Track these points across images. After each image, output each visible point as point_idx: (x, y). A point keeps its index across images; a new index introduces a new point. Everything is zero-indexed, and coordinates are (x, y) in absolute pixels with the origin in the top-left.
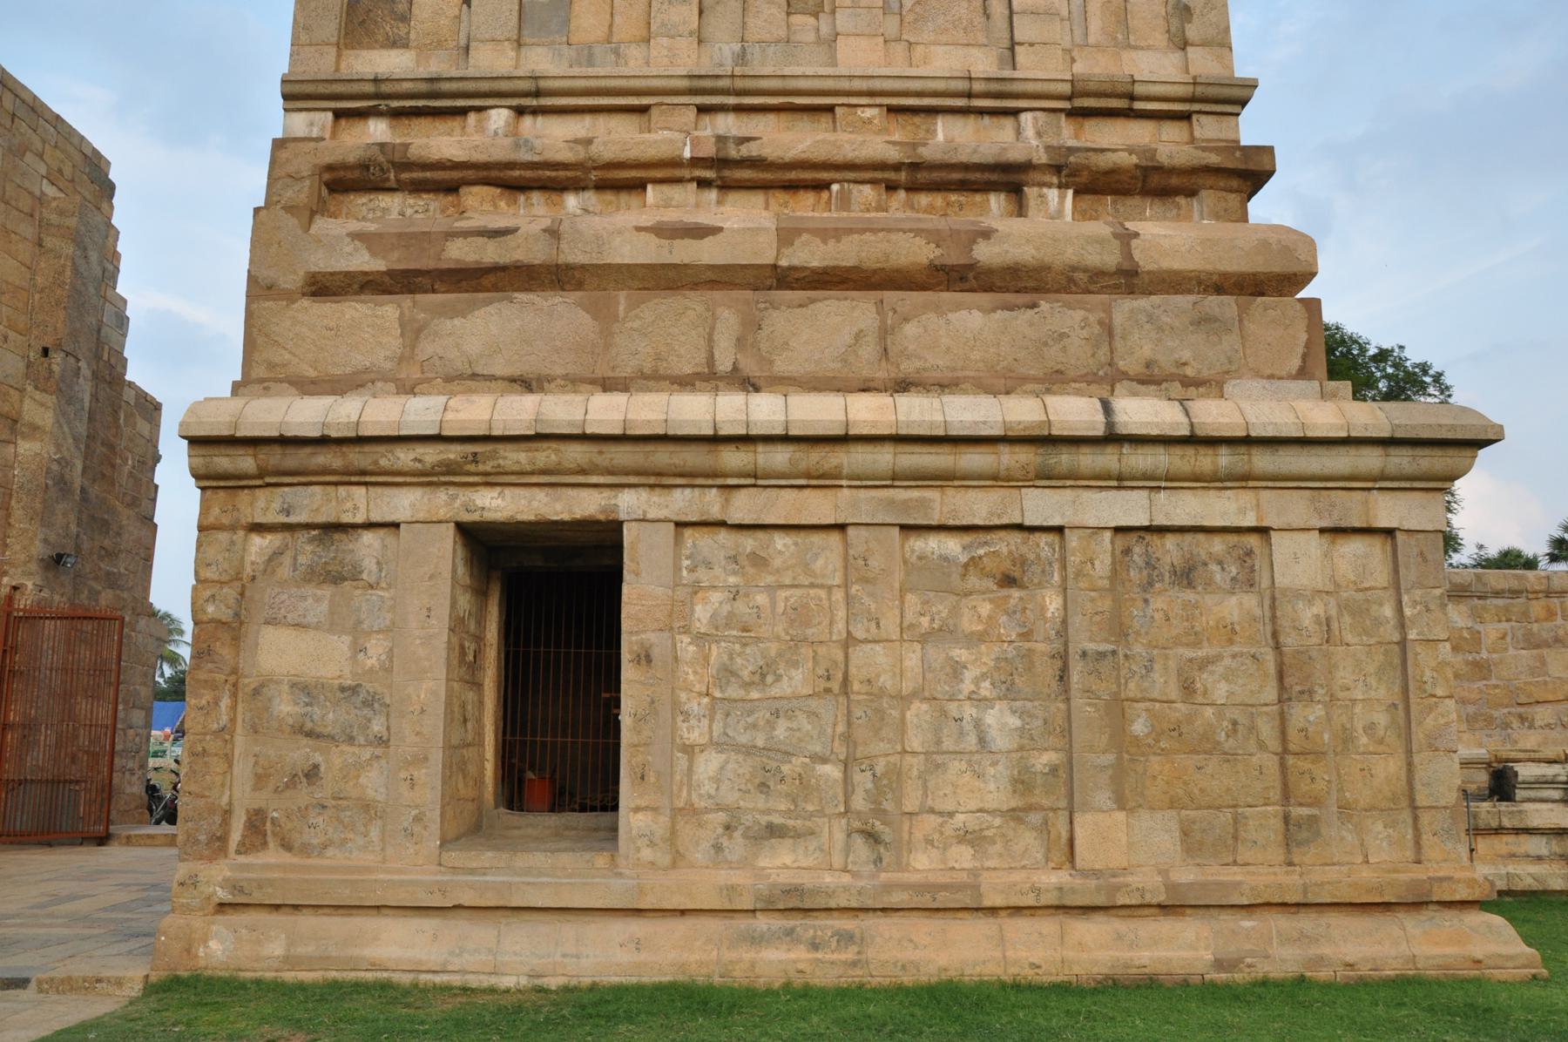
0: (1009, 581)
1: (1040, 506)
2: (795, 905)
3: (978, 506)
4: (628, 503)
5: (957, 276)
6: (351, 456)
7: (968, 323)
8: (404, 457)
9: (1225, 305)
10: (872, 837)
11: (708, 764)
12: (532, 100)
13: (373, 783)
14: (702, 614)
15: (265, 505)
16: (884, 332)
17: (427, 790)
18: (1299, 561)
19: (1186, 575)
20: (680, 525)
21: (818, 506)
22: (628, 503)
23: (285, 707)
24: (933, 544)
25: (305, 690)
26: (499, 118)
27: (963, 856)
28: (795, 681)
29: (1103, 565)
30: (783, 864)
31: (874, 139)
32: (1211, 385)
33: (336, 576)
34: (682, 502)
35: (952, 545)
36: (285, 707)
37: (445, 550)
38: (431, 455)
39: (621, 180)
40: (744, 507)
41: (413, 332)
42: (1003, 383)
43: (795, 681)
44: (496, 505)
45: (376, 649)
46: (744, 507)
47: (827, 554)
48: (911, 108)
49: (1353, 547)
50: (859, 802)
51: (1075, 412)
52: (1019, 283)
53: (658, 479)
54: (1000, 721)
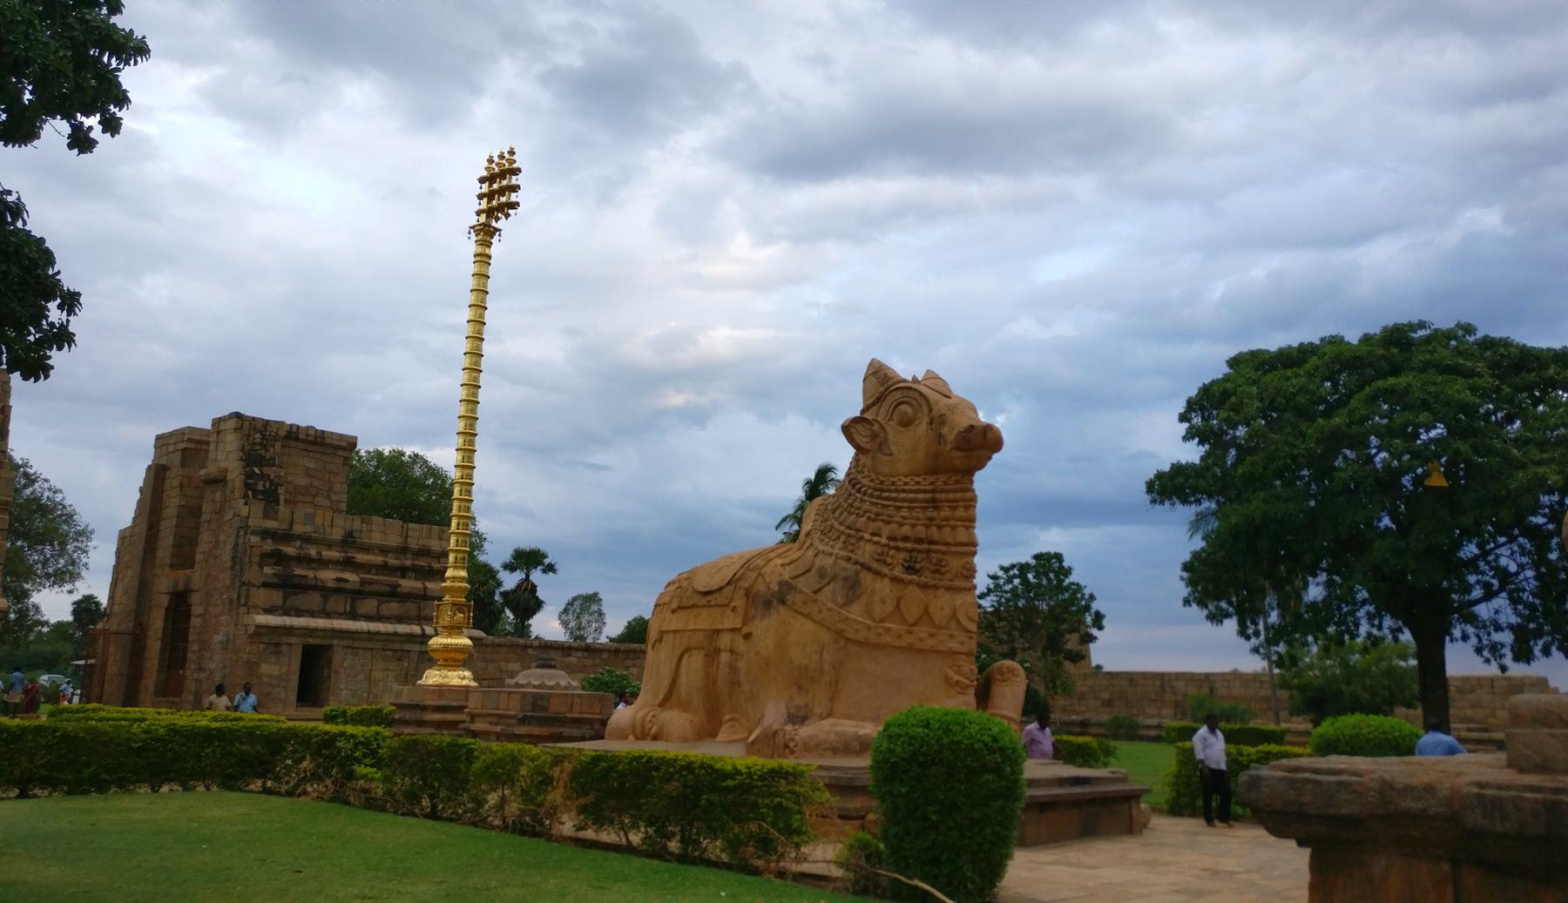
1: (407, 647)
3: (397, 646)
4: (335, 642)
5: (393, 594)
6: (289, 630)
7: (393, 607)
12: (307, 539)
13: (283, 695)
15: (266, 639)
17: (293, 697)
21: (369, 645)
22: (335, 642)
23: (266, 680)
25: (270, 676)
26: (298, 543)
28: (361, 677)
31: (378, 559)
33: (278, 653)
34: (345, 642)
36: (266, 680)
39: (323, 563)
40: (356, 644)
41: (285, 598)
43: (361, 677)
44: (311, 641)
45: (285, 669)
46: (356, 644)
47: (369, 655)
48: (384, 551)
51: (416, 629)
52: (405, 597)
53: (342, 638)
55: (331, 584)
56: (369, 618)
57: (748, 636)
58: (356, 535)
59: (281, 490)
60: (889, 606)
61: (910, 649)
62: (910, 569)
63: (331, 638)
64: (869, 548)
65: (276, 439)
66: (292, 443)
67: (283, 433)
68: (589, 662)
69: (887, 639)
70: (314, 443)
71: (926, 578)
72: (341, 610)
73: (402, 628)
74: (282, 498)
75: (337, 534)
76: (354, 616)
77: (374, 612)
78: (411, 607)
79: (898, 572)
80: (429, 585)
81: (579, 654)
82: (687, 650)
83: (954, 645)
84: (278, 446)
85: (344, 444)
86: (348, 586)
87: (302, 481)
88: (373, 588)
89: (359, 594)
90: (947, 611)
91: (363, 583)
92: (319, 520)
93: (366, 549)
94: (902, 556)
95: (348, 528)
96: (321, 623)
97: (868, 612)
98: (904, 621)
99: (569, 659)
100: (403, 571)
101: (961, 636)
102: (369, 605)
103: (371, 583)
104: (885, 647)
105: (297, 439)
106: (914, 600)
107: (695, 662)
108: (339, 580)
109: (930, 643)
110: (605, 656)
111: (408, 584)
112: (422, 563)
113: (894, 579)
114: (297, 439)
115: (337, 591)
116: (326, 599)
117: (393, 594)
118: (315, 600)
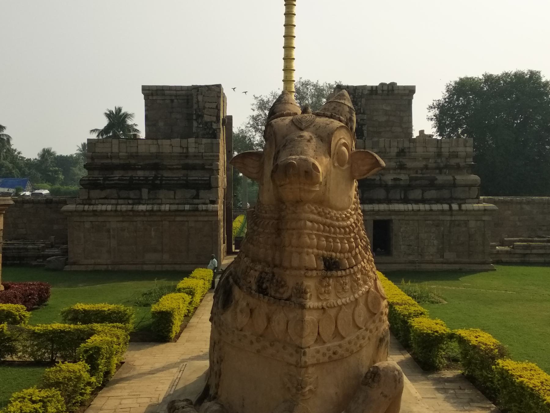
0: (437, 226)
1: (441, 217)
2: (412, 262)
4: (393, 217)
8: (368, 213)
9: (467, 189)
10: (421, 255)
11: (403, 247)
14: (402, 230)
16: (423, 193)
18: (472, 224)
19: (459, 225)
20: (399, 220)
22: (393, 217)
24: (428, 222)
27: (431, 257)
29: (448, 224)
30: (411, 258)
32: (463, 201)
35: (431, 222)
37: (372, 222)
38: (372, 213)
42: (438, 201)
44: (378, 218)
48: (427, 159)
49: (479, 222)
50: (420, 251)
52: (440, 187)
54: (435, 242)
55: (390, 183)
56: (417, 202)
58: (407, 150)
59: (365, 128)
63: (390, 215)
65: (361, 97)
66: (374, 97)
67: (366, 92)
70: (388, 95)
72: (398, 197)
73: (435, 207)
74: (365, 132)
75: (394, 151)
76: (406, 201)
77: (420, 197)
78: (446, 193)
80: (458, 177)
84: (363, 101)
85: (407, 92)
86: (402, 183)
87: (383, 119)
88: (418, 182)
89: (408, 187)
91: (411, 179)
92: (382, 145)
93: (414, 159)
95: (401, 146)
96: (383, 207)
100: (440, 169)
102: (416, 194)
103: (416, 179)
105: (376, 94)
108: (395, 179)
111: (441, 179)
112: (453, 162)
114: (376, 94)
115: (395, 187)
116: (388, 192)
117: (432, 184)
118: (381, 193)
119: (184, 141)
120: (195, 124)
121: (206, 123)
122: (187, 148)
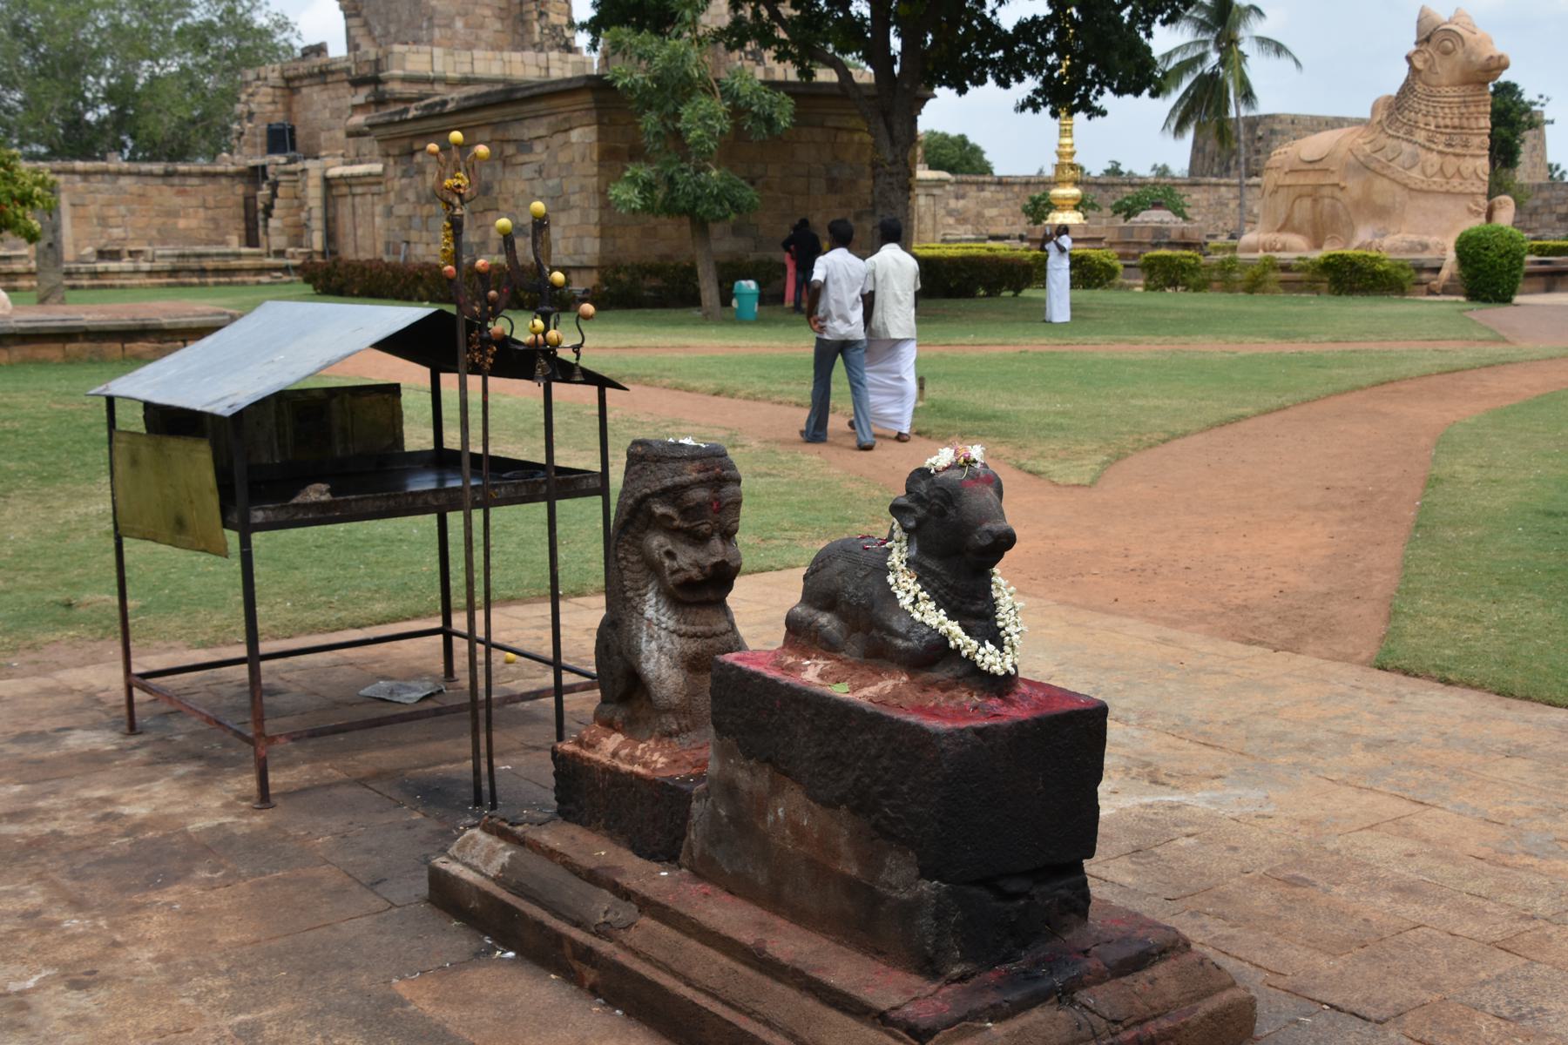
57: (1343, 189)
60: (1437, 167)
61: (1447, 192)
62: (1449, 145)
64: (1423, 133)
68: (1001, 196)
69: (1434, 187)
71: (1458, 150)
79: (1441, 147)
81: (993, 188)
82: (1300, 196)
83: (1474, 189)
90: (1471, 169)
94: (1443, 138)
97: (1424, 172)
98: (1444, 176)
99: (983, 194)
101: (1479, 183)
104: (1433, 192)
106: (1451, 164)
107: (1307, 203)
109: (1460, 188)
110: (1016, 189)
113: (1440, 152)
119: (542, 56)
120: (537, 28)
121: (554, 27)
122: (548, 69)
